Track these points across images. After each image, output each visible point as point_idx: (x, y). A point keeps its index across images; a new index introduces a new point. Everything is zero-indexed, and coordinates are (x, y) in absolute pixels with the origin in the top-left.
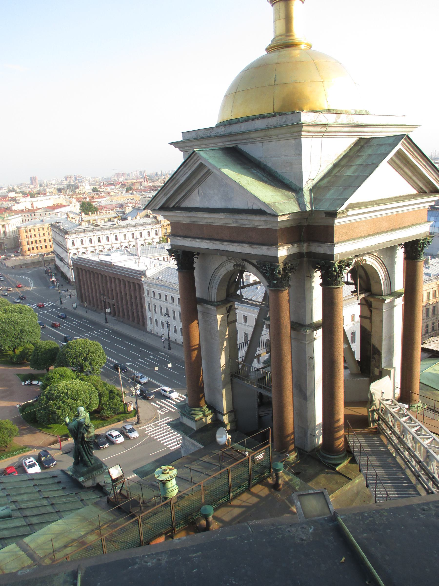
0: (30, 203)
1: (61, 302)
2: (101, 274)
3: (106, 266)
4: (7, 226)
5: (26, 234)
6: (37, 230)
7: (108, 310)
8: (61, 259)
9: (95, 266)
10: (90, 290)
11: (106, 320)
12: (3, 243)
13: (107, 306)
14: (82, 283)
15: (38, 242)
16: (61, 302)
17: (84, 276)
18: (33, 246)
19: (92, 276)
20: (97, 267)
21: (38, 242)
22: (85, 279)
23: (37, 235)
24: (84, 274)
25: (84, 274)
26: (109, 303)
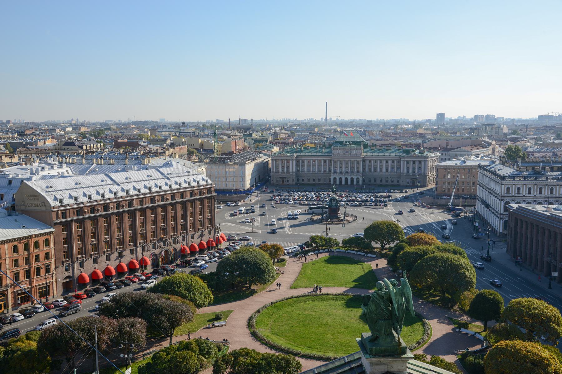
0: (446, 142)
1: (488, 252)
2: (549, 230)
3: (559, 222)
4: (423, 163)
7: (555, 274)
8: (487, 206)
9: (543, 220)
10: (529, 246)
11: (550, 285)
13: (552, 269)
14: (518, 236)
16: (488, 252)
17: (524, 229)
19: (535, 230)
20: (545, 221)
22: (523, 233)
24: (524, 226)
25: (524, 226)
26: (555, 267)
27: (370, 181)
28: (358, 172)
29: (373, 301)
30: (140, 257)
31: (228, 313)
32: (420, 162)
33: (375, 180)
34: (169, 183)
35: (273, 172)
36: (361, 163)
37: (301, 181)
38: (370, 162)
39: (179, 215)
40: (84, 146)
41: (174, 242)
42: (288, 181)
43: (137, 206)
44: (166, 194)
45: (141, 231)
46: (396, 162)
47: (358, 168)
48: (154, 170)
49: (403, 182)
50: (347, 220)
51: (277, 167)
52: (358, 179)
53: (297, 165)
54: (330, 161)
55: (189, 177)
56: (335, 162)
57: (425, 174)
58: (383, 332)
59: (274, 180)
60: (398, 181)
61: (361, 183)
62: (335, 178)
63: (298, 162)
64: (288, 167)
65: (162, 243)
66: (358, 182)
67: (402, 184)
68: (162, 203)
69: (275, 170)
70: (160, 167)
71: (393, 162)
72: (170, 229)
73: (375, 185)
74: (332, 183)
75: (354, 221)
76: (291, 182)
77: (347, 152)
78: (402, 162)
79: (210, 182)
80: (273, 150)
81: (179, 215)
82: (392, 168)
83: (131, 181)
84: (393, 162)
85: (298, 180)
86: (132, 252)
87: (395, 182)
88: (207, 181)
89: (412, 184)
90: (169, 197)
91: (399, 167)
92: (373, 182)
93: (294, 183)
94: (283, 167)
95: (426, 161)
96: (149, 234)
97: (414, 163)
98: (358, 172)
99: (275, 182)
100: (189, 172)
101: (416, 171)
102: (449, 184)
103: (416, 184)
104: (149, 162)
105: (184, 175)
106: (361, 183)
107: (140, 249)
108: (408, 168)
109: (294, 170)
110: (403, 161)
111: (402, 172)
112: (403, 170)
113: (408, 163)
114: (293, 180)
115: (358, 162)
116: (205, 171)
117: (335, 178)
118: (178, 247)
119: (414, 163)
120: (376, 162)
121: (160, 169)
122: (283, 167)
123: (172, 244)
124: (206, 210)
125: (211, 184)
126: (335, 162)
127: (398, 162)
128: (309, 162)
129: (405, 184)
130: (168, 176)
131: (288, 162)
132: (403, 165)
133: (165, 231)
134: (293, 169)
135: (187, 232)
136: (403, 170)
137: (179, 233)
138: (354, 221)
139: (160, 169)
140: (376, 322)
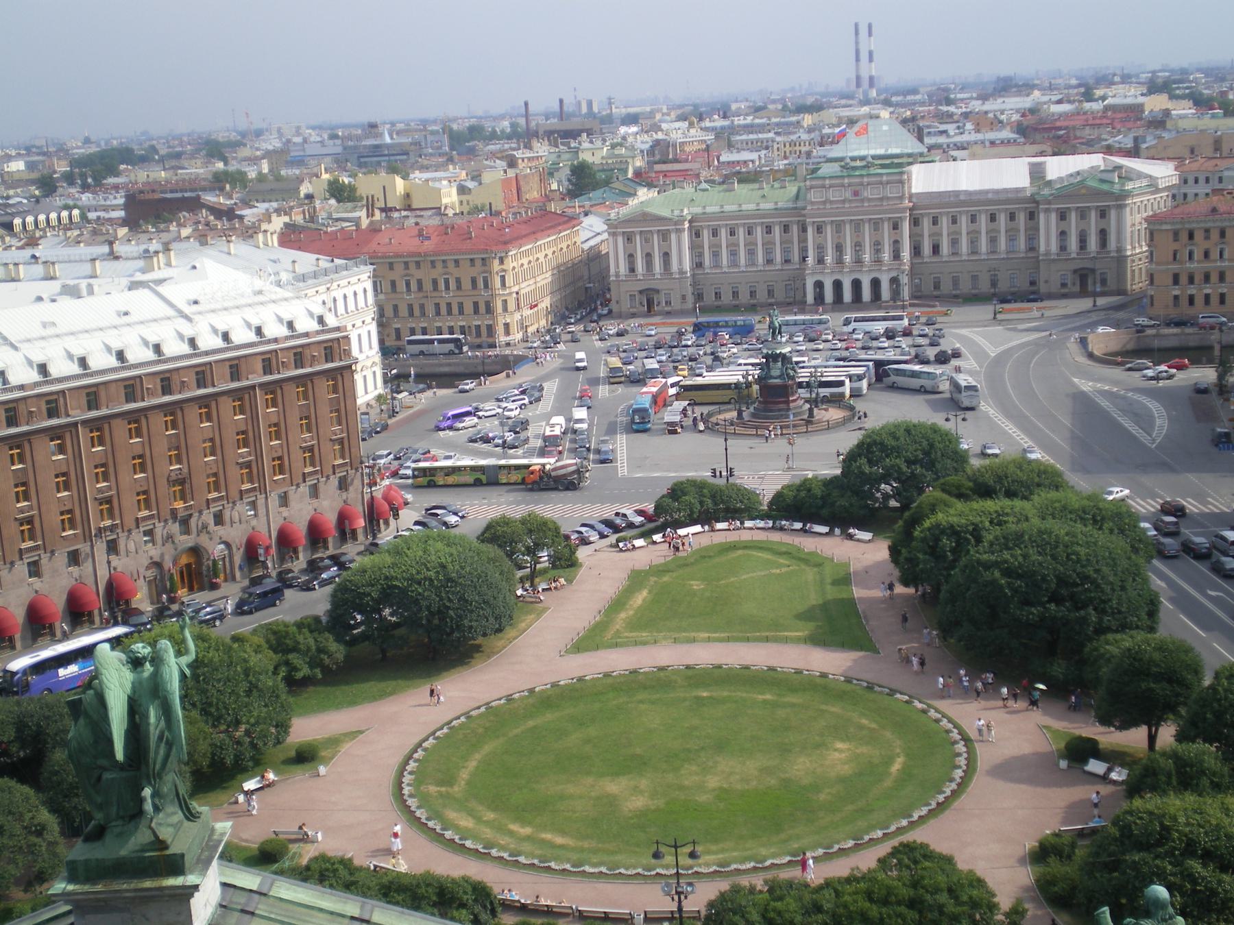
4: (1113, 214)
5: (1176, 246)
6: (1215, 235)
12: (1093, 271)
15: (1214, 278)
18: (1192, 290)
21: (1214, 278)
23: (1215, 254)
27: (937, 286)
28: (896, 256)
29: (87, 716)
30: (103, 575)
31: (334, 742)
32: (1103, 214)
33: (956, 282)
34: (188, 331)
35: (617, 275)
36: (906, 226)
37: (709, 299)
38: (935, 221)
39: (230, 436)
40: (17, 221)
41: (219, 519)
42: (668, 303)
43: (78, 414)
44: (178, 369)
45: (100, 490)
46: (1021, 218)
47: (896, 243)
48: (143, 293)
49: (1050, 278)
50: (820, 422)
51: (631, 257)
52: (894, 281)
53: (696, 249)
54: (804, 230)
55: (259, 308)
56: (819, 229)
57: (1120, 250)
58: (114, 810)
59: (621, 296)
60: (1033, 283)
61: (906, 293)
62: (819, 285)
63: (698, 235)
64: (666, 256)
65: (175, 528)
66: (896, 294)
67: (1043, 288)
68: (167, 399)
69: (623, 269)
70: (160, 282)
71: (1012, 217)
72: (200, 481)
73: (956, 296)
74: (810, 298)
75: (845, 421)
76: (676, 304)
77: (856, 194)
78: (1042, 216)
79: (331, 321)
80: (633, 202)
81: (230, 436)
82: (1012, 239)
83: (58, 331)
84: (1012, 217)
85: (699, 297)
86: (74, 558)
87: (1022, 284)
88: (321, 320)
89: (1077, 288)
90: (190, 378)
91: (1032, 238)
92: (946, 287)
93: (690, 305)
94: (648, 257)
95: (1121, 207)
96: (129, 500)
97: (1083, 214)
98: (896, 256)
99: (626, 305)
100: (260, 292)
101: (1093, 243)
102: (1191, 280)
103: (1090, 288)
104: (169, 264)
105: (243, 301)
106: (906, 293)
107: (100, 547)
108: (1063, 234)
109: (687, 266)
110: (1047, 211)
111: (1042, 249)
112: (1048, 243)
113: (1063, 216)
114: (684, 297)
115: (896, 227)
116: (369, 285)
117: (819, 285)
118: (236, 534)
119: (1083, 214)
120: (954, 221)
121: (159, 289)
122: (648, 257)
123: (212, 527)
124: (325, 411)
125: (338, 329)
126: (819, 229)
127: (1032, 216)
128: (732, 233)
129: (1055, 287)
130: (188, 310)
131: (665, 236)
132: (1048, 225)
133: (182, 484)
134: (683, 260)
135: (263, 489)
136: (1048, 243)
137: (234, 494)
138: (845, 421)
139: (159, 289)
140: (99, 779)
